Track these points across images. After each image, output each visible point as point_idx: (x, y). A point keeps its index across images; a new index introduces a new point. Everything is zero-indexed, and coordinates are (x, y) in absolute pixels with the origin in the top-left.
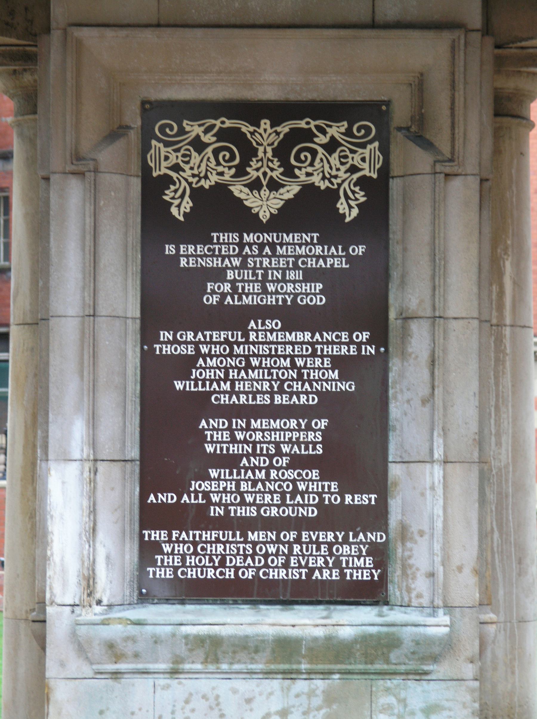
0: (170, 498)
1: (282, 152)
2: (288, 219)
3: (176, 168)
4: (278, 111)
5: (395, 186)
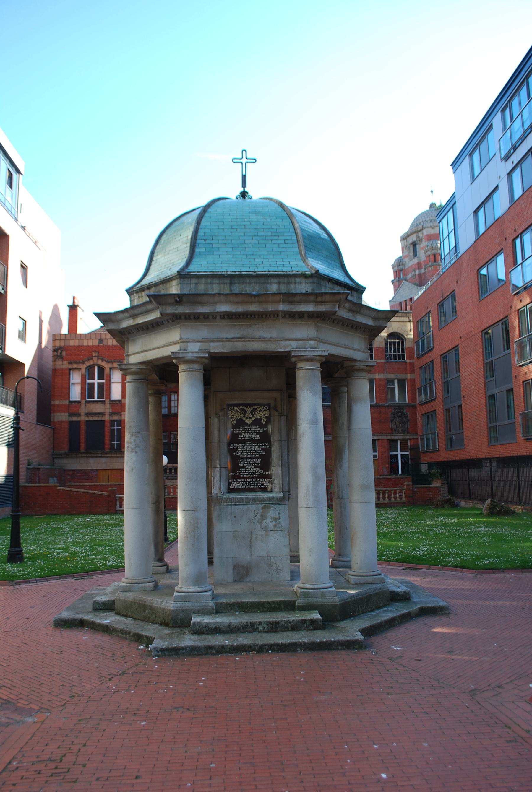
0: (234, 474)
1: (252, 412)
2: (252, 424)
3: (233, 415)
4: (250, 405)
5: (272, 418)
